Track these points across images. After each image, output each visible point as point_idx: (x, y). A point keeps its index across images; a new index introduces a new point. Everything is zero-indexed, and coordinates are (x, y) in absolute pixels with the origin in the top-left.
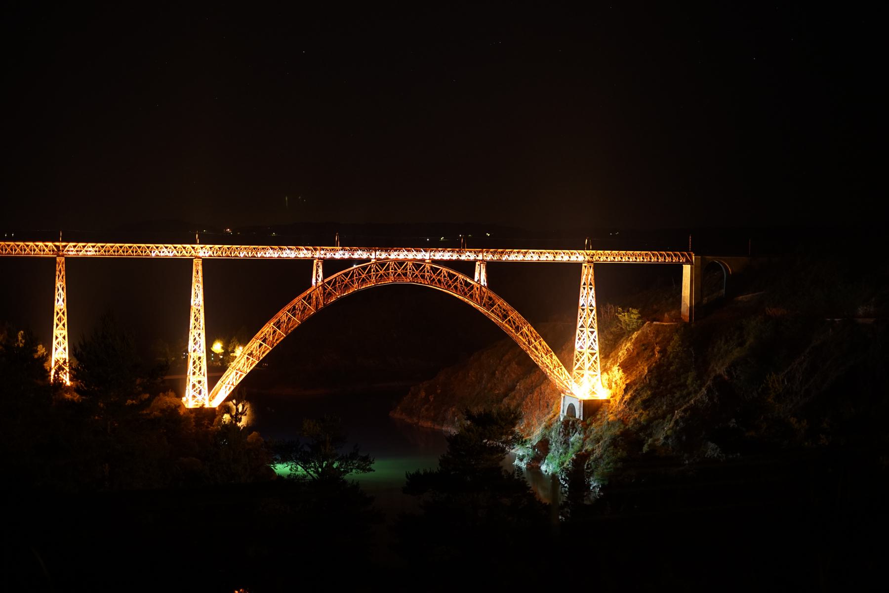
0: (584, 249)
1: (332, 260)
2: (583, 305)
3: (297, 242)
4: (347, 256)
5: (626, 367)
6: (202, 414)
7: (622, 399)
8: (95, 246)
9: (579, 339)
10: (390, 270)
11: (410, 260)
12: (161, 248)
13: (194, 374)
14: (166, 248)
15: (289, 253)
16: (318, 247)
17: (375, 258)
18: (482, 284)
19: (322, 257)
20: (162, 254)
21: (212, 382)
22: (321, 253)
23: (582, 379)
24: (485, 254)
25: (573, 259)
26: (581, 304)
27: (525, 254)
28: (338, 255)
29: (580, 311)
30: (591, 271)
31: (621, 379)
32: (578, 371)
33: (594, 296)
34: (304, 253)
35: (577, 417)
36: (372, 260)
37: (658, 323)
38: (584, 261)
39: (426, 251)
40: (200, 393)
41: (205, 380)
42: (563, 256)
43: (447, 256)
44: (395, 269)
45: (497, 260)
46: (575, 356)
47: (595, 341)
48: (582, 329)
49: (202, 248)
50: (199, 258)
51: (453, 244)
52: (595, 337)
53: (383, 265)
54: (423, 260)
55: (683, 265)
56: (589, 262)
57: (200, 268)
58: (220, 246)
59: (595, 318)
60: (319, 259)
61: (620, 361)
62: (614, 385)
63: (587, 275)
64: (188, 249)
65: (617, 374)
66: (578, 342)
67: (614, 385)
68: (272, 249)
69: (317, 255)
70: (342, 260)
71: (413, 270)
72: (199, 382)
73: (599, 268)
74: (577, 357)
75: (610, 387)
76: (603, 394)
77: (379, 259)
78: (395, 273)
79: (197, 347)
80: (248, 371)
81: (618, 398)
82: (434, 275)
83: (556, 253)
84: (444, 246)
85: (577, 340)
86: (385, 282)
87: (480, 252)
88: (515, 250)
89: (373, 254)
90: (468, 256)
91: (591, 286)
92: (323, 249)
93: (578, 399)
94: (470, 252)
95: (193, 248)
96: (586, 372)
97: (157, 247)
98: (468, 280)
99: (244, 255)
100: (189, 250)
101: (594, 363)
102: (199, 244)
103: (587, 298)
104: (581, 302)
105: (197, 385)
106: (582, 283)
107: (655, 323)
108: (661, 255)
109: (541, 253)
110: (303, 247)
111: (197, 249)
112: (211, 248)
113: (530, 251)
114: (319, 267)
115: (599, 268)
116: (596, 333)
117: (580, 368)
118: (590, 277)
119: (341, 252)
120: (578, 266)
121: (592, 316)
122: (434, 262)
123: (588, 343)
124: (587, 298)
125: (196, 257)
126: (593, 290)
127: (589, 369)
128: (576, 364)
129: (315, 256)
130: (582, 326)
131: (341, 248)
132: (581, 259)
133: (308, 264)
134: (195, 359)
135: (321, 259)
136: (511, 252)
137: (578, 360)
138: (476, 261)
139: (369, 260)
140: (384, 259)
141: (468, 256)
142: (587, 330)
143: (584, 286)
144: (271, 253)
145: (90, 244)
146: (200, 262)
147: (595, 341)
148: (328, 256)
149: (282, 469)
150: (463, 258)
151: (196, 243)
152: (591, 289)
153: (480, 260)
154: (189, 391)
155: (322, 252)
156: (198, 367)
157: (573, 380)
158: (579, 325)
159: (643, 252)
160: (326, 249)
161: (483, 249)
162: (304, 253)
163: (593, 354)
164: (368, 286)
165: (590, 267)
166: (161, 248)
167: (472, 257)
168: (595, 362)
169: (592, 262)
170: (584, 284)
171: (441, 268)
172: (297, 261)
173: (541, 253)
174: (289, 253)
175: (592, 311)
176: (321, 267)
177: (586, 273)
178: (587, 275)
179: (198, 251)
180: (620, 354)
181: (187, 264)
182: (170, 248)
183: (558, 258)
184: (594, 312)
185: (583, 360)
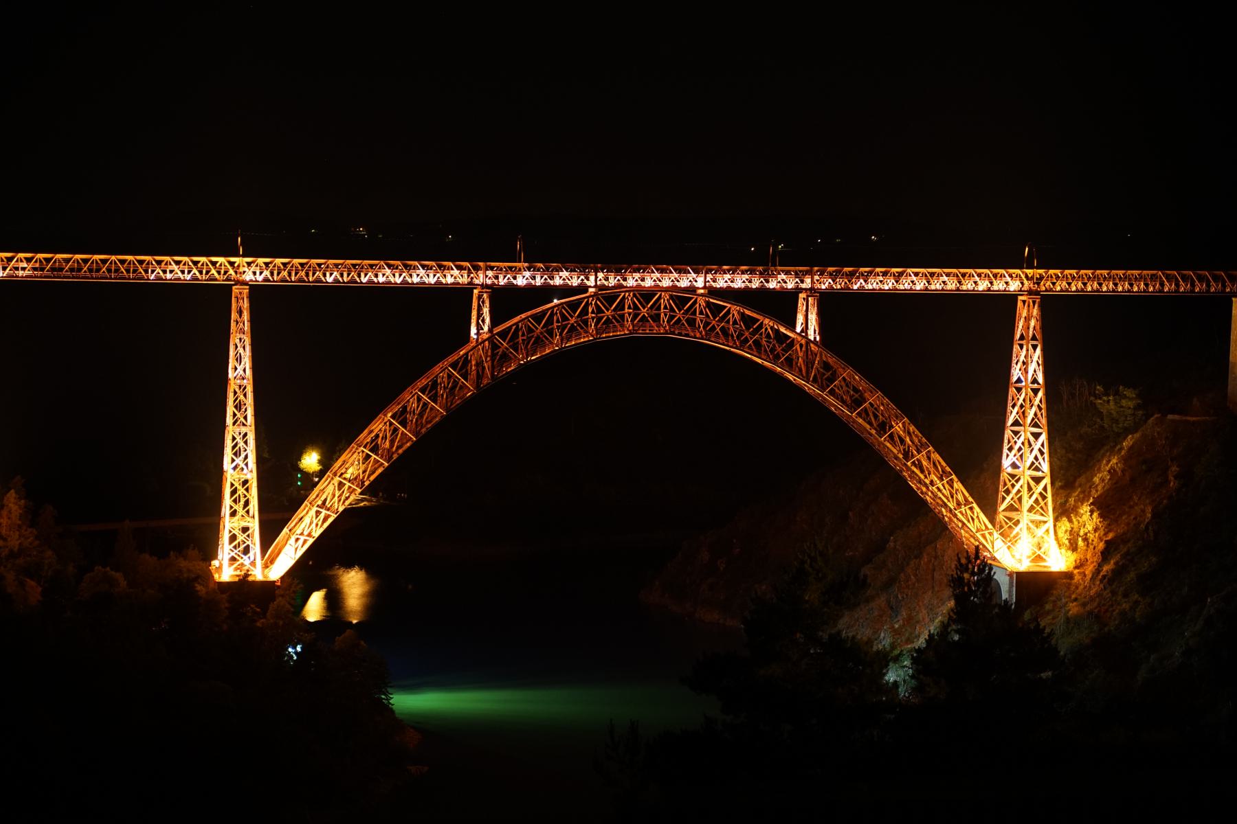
1: (511, 288)
2: (1019, 380)
3: (439, 255)
4: (539, 282)
5: (1104, 507)
7: (1097, 571)
8: (32, 258)
9: (1010, 449)
10: (626, 310)
11: (667, 290)
12: (166, 264)
13: (233, 514)
14: (178, 263)
15: (422, 276)
16: (481, 264)
17: (596, 286)
18: (812, 338)
19: (489, 282)
20: (169, 276)
21: (271, 531)
23: (1017, 529)
24: (817, 277)
25: (999, 286)
26: (1015, 379)
27: (898, 277)
28: (520, 281)
29: (1012, 391)
30: (1035, 312)
31: (1096, 530)
32: (1008, 514)
33: (1040, 362)
34: (453, 276)
36: (591, 290)
37: (1176, 417)
38: (1020, 291)
39: (697, 272)
40: (246, 551)
41: (255, 525)
42: (978, 282)
43: (739, 282)
44: (636, 308)
45: (842, 289)
46: (1002, 483)
47: (1042, 453)
49: (249, 264)
50: (244, 283)
52: (1043, 445)
53: (610, 299)
54: (692, 290)
55: (1234, 299)
56: (1030, 292)
57: (246, 305)
59: (1043, 406)
60: (484, 286)
62: (1080, 543)
63: (1028, 319)
64: (221, 265)
65: (1088, 520)
66: (1008, 455)
67: (1080, 543)
68: (389, 266)
69: (480, 279)
70: (530, 289)
71: (672, 310)
72: (245, 530)
73: (1051, 306)
74: (1005, 484)
75: (1073, 547)
76: (1059, 561)
77: (602, 288)
78: (636, 316)
79: (239, 461)
80: (341, 509)
81: (1089, 570)
82: (714, 318)
83: (964, 275)
84: (734, 261)
85: (1005, 451)
86: (615, 334)
87: (807, 273)
88: (878, 270)
89: (592, 278)
90: (782, 281)
91: (1035, 343)
92: (492, 268)
93: (1006, 569)
94: (787, 273)
95: (232, 264)
96: (1025, 518)
97: (159, 263)
98: (783, 330)
99: (334, 279)
100: (223, 267)
101: (1040, 499)
102: (244, 256)
104: (1016, 373)
105: (241, 537)
106: (1018, 336)
107: (1170, 417)
108: (1185, 278)
109: (932, 275)
111: (239, 266)
112: (267, 264)
113: (909, 270)
114: (483, 302)
115: (1051, 306)
116: (1043, 437)
117: (1011, 508)
118: (1033, 323)
119: (527, 274)
120: (1009, 301)
121: (1037, 402)
122: (713, 292)
123: (1030, 459)
125: (238, 282)
127: (1031, 509)
128: (1004, 499)
129: (476, 281)
130: (1016, 423)
131: (526, 264)
132: (1014, 286)
133: (462, 295)
134: (236, 485)
135: (487, 286)
136: (871, 272)
137: (1008, 492)
138: (798, 291)
139: (583, 289)
140: (614, 287)
141: (782, 281)
142: (1026, 432)
144: (386, 275)
145: (21, 255)
147: (1042, 453)
150: (772, 285)
151: (237, 255)
152: (1035, 347)
153: (806, 290)
154: (225, 550)
155: (490, 273)
156: (243, 501)
157: (996, 535)
159: (1145, 272)
160: (498, 267)
161: (812, 266)
162: (453, 276)
164: (582, 340)
165: (1034, 303)
166: (166, 264)
167: (790, 285)
168: (1044, 498)
169: (1037, 293)
170: (1022, 338)
171: (729, 305)
173: (932, 275)
174: (422, 276)
175: (1036, 391)
176: (487, 304)
177: (1024, 314)
178: (1028, 319)
179: (241, 270)
180: (1096, 480)
181: (219, 295)
182: (184, 264)
183: (968, 286)
185: (1019, 491)
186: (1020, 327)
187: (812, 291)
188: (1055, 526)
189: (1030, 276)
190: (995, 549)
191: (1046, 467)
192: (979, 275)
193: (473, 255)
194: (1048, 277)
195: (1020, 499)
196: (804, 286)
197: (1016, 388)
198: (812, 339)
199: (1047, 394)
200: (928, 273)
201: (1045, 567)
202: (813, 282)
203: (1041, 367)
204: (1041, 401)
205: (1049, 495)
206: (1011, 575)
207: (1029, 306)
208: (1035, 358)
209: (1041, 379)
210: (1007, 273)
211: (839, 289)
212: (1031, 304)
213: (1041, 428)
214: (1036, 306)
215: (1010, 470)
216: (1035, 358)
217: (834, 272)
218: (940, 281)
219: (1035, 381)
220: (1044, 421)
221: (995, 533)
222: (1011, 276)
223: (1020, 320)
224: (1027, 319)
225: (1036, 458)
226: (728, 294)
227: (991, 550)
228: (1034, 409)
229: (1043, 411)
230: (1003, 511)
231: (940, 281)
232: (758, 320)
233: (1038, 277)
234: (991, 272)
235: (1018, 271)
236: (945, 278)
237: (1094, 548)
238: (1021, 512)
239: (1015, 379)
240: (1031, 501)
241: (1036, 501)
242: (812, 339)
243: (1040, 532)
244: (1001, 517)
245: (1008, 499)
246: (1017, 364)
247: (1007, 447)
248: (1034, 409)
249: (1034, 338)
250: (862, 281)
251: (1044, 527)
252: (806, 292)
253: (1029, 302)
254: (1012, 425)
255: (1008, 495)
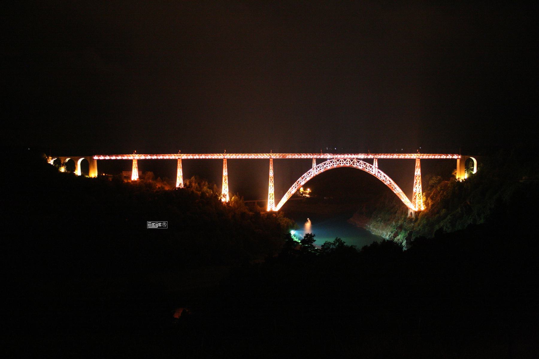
0: (416, 153)
3: (306, 152)
6: (272, 213)
15: (304, 156)
16: (314, 154)
19: (316, 157)
21: (277, 202)
22: (315, 156)
34: (309, 156)
35: (413, 217)
36: (335, 158)
39: (354, 155)
42: (408, 156)
49: (273, 155)
50: (272, 158)
51: (366, 152)
56: (418, 158)
57: (272, 163)
58: (285, 154)
63: (418, 164)
73: (422, 161)
85: (414, 188)
90: (370, 156)
94: (372, 155)
102: (272, 153)
103: (418, 172)
104: (416, 174)
106: (416, 166)
110: (302, 154)
113: (395, 154)
120: (414, 161)
121: (419, 179)
122: (357, 159)
124: (418, 172)
125: (271, 158)
126: (420, 169)
130: (416, 183)
133: (311, 160)
135: (315, 158)
139: (333, 158)
141: (370, 156)
142: (417, 186)
146: (272, 159)
148: (318, 157)
149: (152, 225)
151: (270, 153)
155: (316, 156)
158: (415, 182)
162: (309, 156)
163: (419, 193)
169: (419, 158)
170: (417, 167)
172: (307, 159)
173: (399, 155)
174: (304, 156)
175: (419, 177)
178: (418, 164)
187: (376, 158)
192: (408, 155)
193: (313, 152)
196: (374, 157)
206: (414, 211)
219: (419, 175)
220: (421, 182)
224: (418, 163)
226: (360, 159)
228: (419, 180)
241: (420, 198)
244: (413, 200)
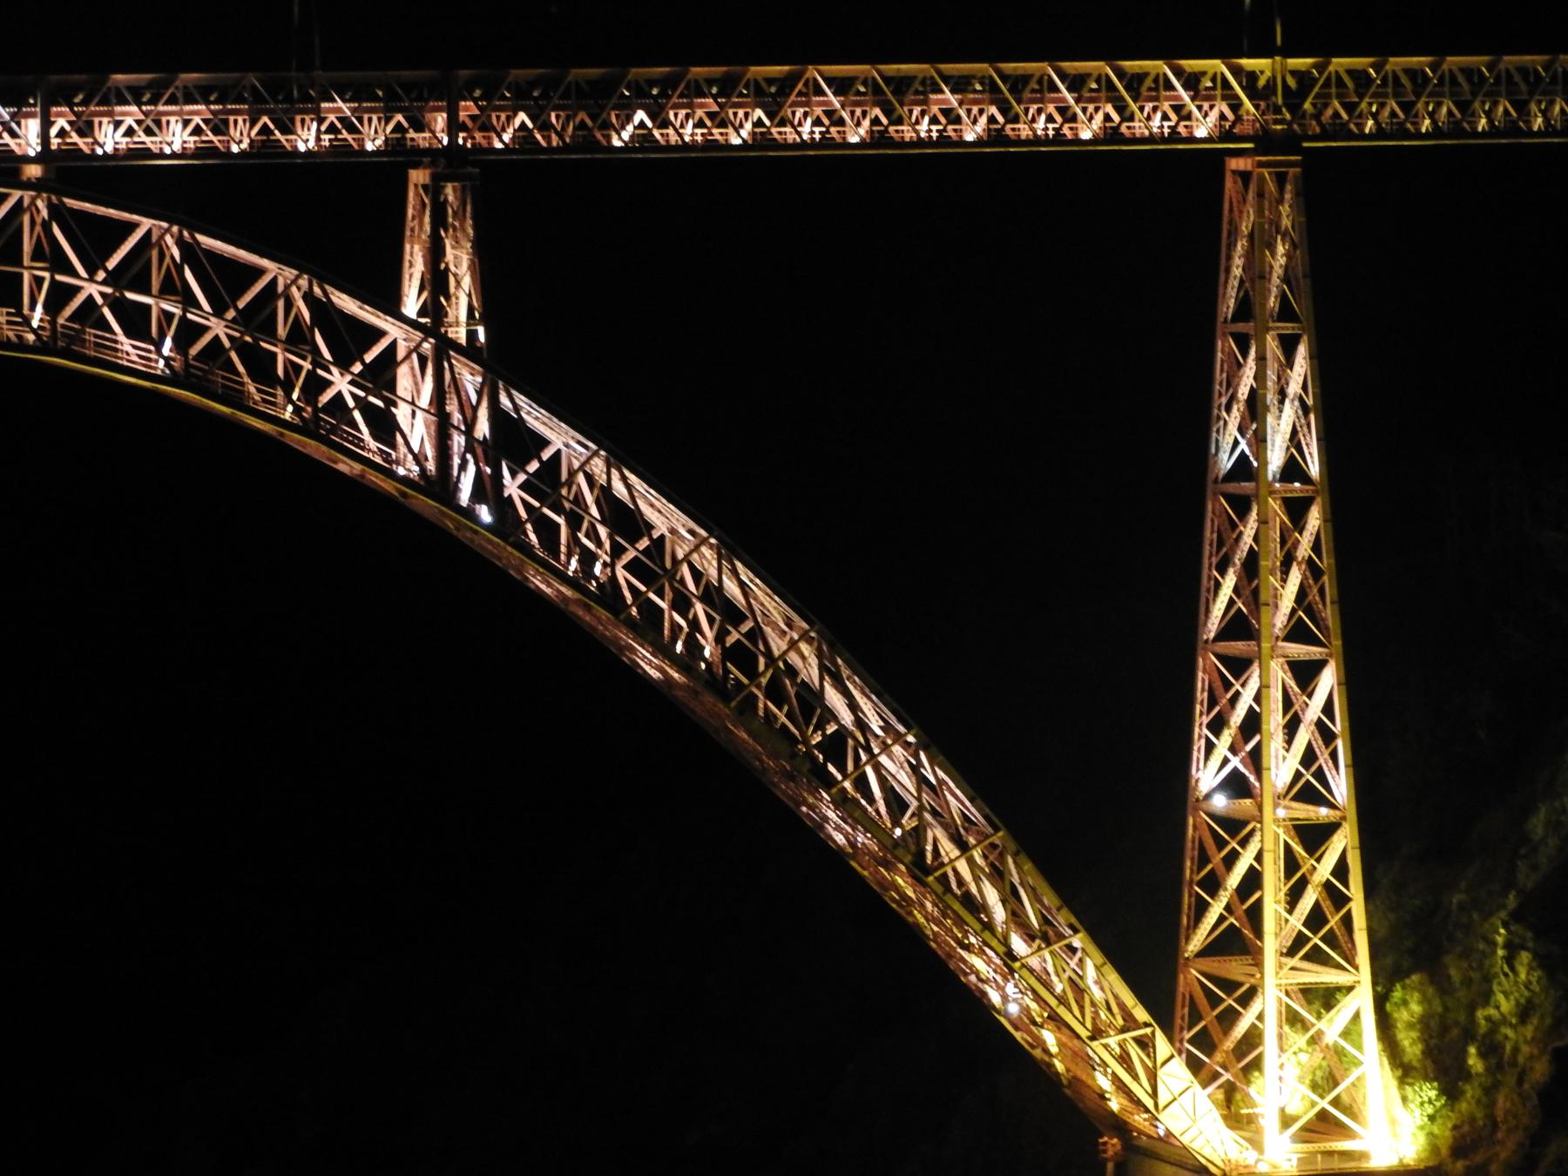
2: (1242, 469)
9: (1217, 726)
18: (460, 334)
26: (1226, 462)
27: (774, 99)
29: (1216, 506)
33: (1310, 402)
38: (1226, 136)
45: (565, 148)
46: (1190, 854)
48: (1238, 647)
56: (1265, 142)
59: (1326, 563)
61: (1527, 878)
62: (1474, 1061)
67: (1474, 1061)
74: (1204, 859)
81: (1506, 1149)
82: (92, 273)
85: (1201, 731)
88: (698, 71)
91: (1289, 328)
98: (347, 303)
101: (1327, 906)
106: (1229, 304)
109: (901, 85)
113: (812, 72)
116: (1328, 680)
118: (1279, 257)
123: (1282, 767)
128: (1201, 908)
130: (1239, 626)
136: (668, 84)
137: (1213, 885)
138: (400, 155)
143: (1241, 327)
147: (1327, 736)
150: (306, 138)
165: (1281, 180)
168: (1339, 900)
170: (1245, 310)
171: (146, 223)
173: (901, 85)
175: (1297, 510)
184: (1314, 519)
186: (1237, 272)
187: (448, 162)
188: (1380, 1002)
189: (1262, 82)
190: (1162, 1102)
191: (1341, 786)
192: (1076, 83)
194: (1327, 84)
195: (1255, 916)
196: (421, 139)
197: (1228, 497)
198: (463, 340)
199: (1334, 518)
200: (887, 80)
201: (1344, 1154)
202: (454, 127)
203: (1312, 417)
204: (1316, 547)
205: (1355, 890)
207: (1260, 195)
208: (1294, 388)
209: (1314, 469)
210: (1179, 73)
211: (558, 150)
212: (1271, 186)
213: (1318, 643)
214: (1289, 187)
215: (1220, 802)
216: (1294, 388)
217: (533, 84)
218: (935, 109)
219: (1292, 470)
220: (1329, 614)
221: (1163, 1046)
222: (1191, 82)
223: (1231, 246)
224: (1260, 242)
225: (1309, 757)
227: (1149, 1103)
228: (1295, 577)
229: (1326, 578)
230: (1203, 953)
231: (935, 109)
232: (259, 272)
233: (1291, 82)
234: (1120, 74)
235: (1217, 65)
236: (952, 99)
237: (1520, 1082)
238: (1260, 951)
239: (1226, 462)
240: (1297, 921)
241: (1315, 919)
242: (463, 340)
243: (1332, 1025)
244: (1192, 976)
245: (1216, 909)
246: (1228, 409)
247: (1206, 720)
248: (1295, 577)
249: (1286, 313)
250: (640, 115)
251: (1345, 1008)
252: (433, 164)
253: (1262, 179)
254: (1222, 635)
255: (1213, 894)
